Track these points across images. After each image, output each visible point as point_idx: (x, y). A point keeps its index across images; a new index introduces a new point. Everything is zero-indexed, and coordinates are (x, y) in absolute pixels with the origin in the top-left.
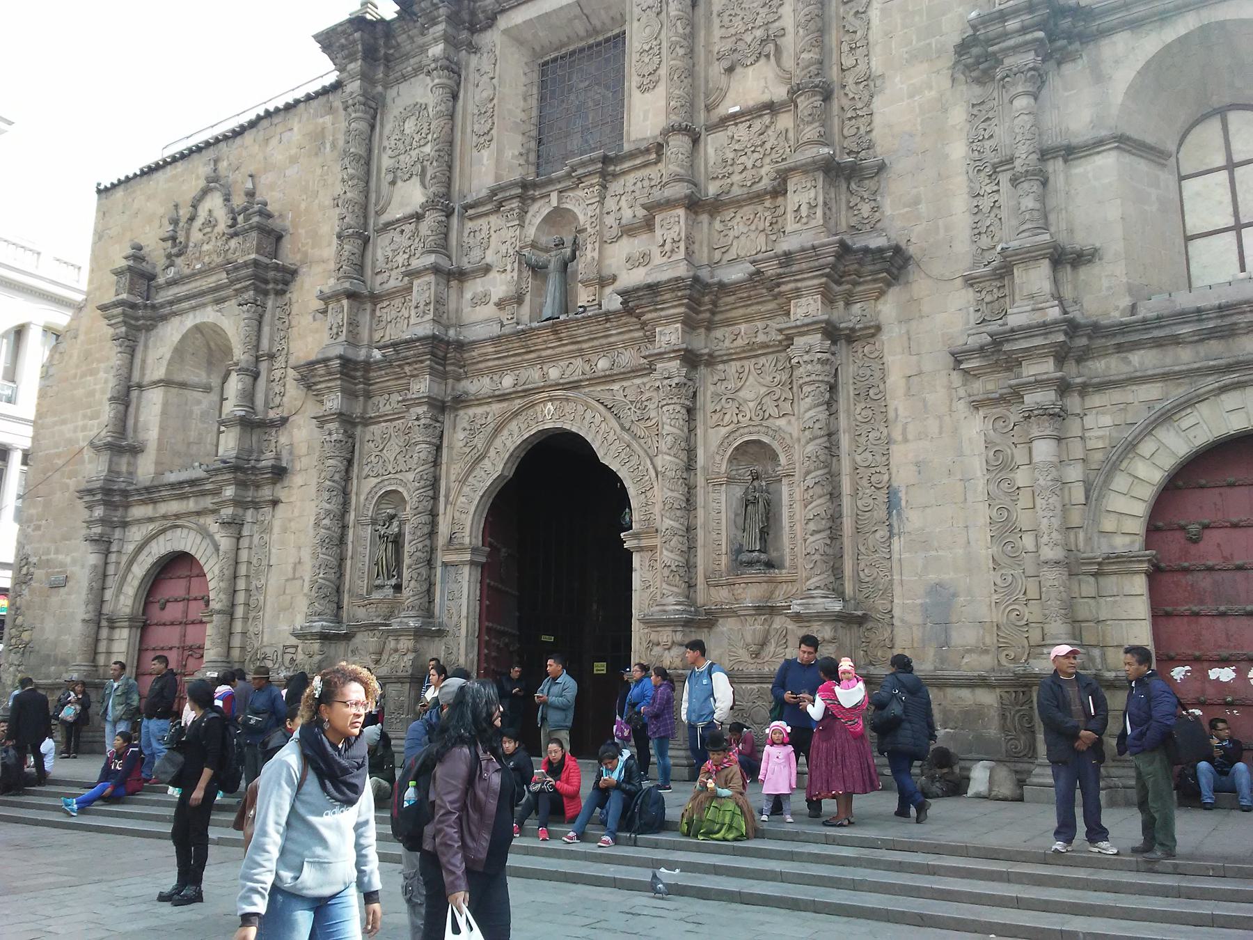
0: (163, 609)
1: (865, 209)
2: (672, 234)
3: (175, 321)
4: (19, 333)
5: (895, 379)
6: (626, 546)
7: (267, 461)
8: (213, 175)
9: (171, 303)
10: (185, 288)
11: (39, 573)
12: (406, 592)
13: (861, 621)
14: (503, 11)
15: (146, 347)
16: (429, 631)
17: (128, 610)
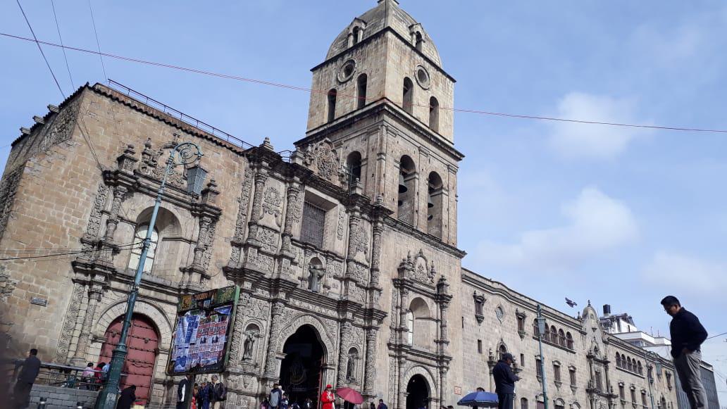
3: (148, 197)
10: (155, 185)
11: (16, 290)
14: (309, 185)
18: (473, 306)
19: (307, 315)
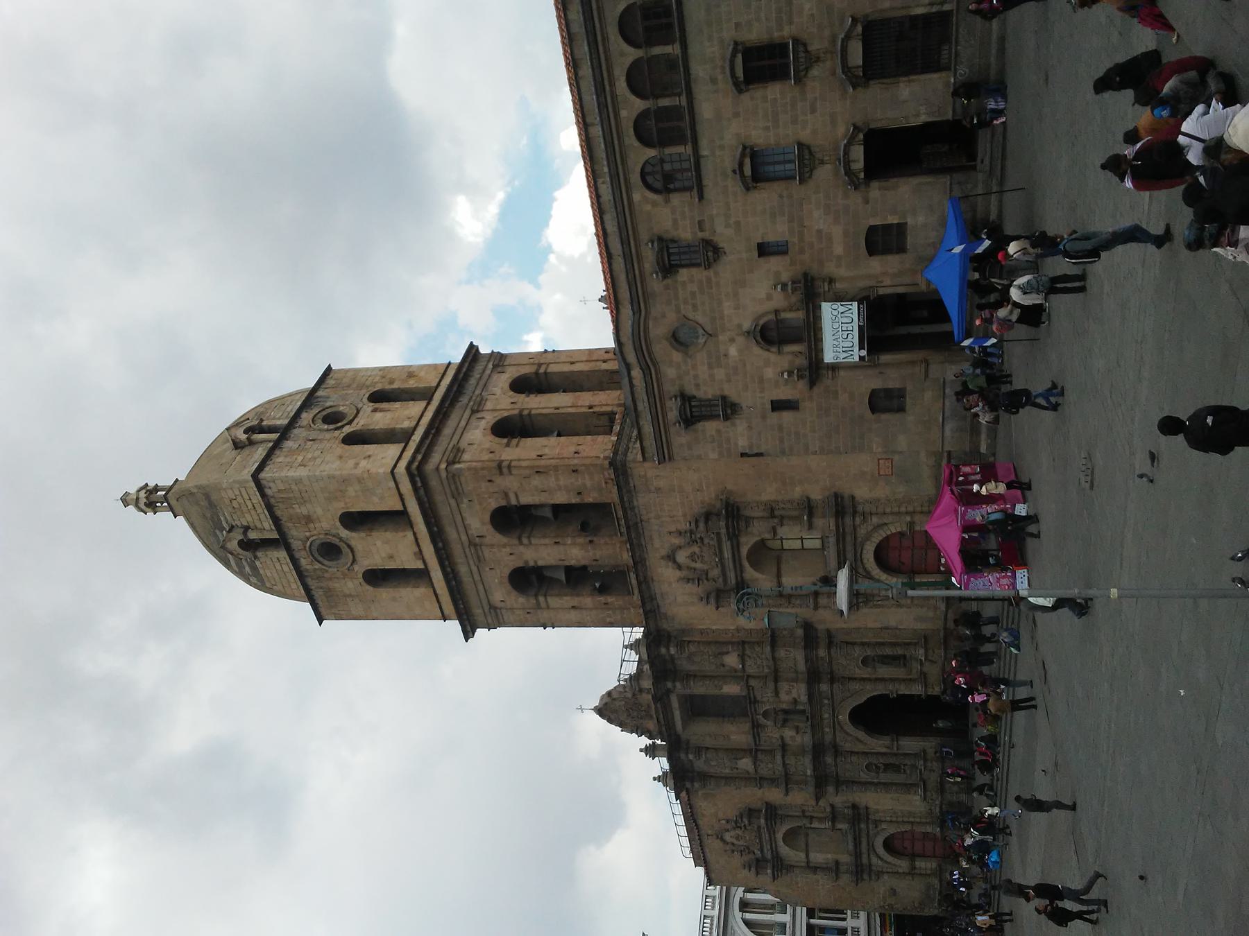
0: (906, 848)
1: (785, 632)
2: (787, 687)
3: (779, 849)
4: (748, 924)
5: (845, 626)
6: (895, 696)
7: (850, 812)
8: (714, 836)
9: (772, 852)
12: (909, 763)
13: (925, 638)
15: (788, 861)
16: (923, 755)
17: (908, 863)
18: (710, 427)
19: (839, 723)
